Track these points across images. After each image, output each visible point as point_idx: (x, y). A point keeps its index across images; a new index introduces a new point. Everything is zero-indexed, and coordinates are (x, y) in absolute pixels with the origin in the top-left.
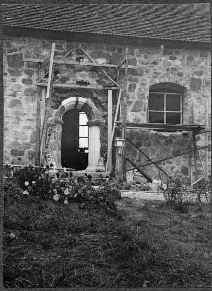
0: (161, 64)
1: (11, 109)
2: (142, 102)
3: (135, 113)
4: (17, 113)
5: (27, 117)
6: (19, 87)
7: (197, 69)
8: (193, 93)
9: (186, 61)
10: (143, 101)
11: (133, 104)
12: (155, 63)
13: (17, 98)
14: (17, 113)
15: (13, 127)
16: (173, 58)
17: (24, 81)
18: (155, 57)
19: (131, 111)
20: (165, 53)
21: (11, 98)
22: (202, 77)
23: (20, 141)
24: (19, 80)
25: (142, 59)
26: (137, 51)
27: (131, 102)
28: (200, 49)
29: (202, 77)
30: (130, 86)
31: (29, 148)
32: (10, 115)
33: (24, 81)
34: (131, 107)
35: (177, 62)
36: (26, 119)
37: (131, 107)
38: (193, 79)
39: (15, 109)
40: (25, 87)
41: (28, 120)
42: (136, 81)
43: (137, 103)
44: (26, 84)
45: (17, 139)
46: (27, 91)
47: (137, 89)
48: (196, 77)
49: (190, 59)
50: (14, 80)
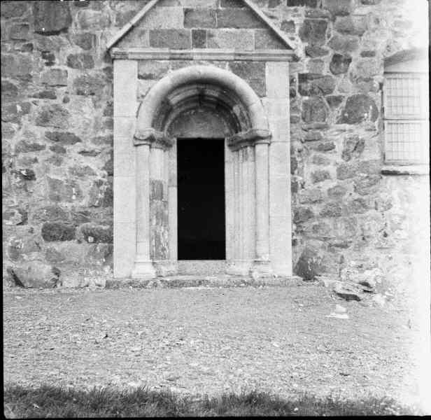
1: (44, 130)
2: (366, 98)
3: (347, 126)
4: (56, 138)
5: (79, 146)
10: (370, 94)
11: (344, 104)
13: (59, 101)
14: (56, 138)
15: (47, 170)
19: (338, 123)
21: (42, 102)
23: (64, 205)
27: (338, 100)
30: (336, 59)
31: (87, 221)
32: (40, 143)
34: (337, 111)
36: (79, 150)
37: (337, 111)
40: (73, 74)
41: (83, 152)
43: (352, 101)
44: (78, 67)
45: (58, 199)
46: (79, 82)
47: (352, 66)
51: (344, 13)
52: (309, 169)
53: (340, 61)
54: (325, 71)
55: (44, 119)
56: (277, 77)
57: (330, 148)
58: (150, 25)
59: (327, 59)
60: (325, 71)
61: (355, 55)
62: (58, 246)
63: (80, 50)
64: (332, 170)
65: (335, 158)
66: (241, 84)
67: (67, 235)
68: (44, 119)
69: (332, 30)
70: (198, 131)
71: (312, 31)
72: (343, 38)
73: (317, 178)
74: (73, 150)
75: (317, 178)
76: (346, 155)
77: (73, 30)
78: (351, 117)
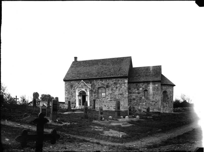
0: (99, 83)
4: (72, 96)
6: (72, 91)
7: (108, 83)
8: (107, 89)
9: (105, 81)
12: (98, 83)
14: (72, 96)
16: (102, 81)
17: (73, 90)
18: (98, 81)
20: (101, 80)
22: (109, 85)
24: (72, 90)
25: (96, 82)
26: (95, 81)
28: (109, 78)
29: (109, 85)
33: (73, 90)
35: (103, 82)
38: (107, 85)
39: (72, 95)
40: (73, 91)
42: (94, 87)
48: (107, 85)
49: (106, 81)
50: (72, 89)
51: (94, 84)
52: (91, 98)
53: (94, 88)
54: (93, 89)
55: (71, 94)
56: (88, 90)
57: (93, 96)
58: (79, 87)
59: (93, 88)
60: (93, 89)
61: (95, 88)
62: (73, 104)
63: (74, 89)
64: (93, 98)
65: (93, 97)
66: (85, 91)
67: (73, 104)
68: (71, 94)
69: (93, 86)
70: (84, 95)
71: (91, 86)
72: (94, 86)
73: (92, 98)
74: (73, 97)
75: (92, 98)
76: (94, 96)
77: (73, 87)
78: (95, 93)
